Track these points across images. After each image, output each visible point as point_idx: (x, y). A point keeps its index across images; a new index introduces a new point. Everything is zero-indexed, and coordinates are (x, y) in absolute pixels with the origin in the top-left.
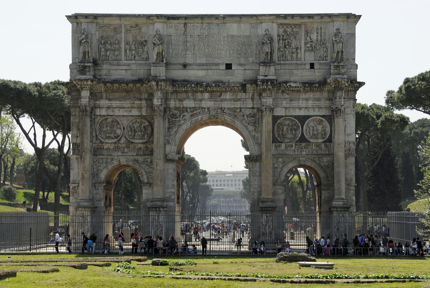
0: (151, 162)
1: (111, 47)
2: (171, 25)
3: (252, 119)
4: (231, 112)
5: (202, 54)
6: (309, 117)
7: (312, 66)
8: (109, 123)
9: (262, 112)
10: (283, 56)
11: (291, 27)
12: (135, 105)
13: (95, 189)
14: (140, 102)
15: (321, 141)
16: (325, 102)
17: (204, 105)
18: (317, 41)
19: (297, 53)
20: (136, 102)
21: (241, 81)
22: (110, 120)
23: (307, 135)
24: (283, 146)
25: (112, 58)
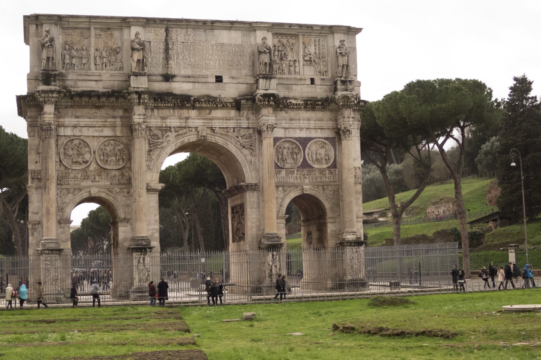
0: (128, 193)
1: (77, 53)
2: (149, 29)
3: (248, 140)
4: (223, 133)
5: (187, 63)
6: (310, 139)
7: (312, 80)
8: (75, 145)
9: (260, 132)
10: (279, 69)
11: (287, 37)
12: (108, 123)
13: (61, 227)
14: (114, 120)
15: (325, 166)
16: (328, 122)
17: (191, 124)
18: (316, 54)
19: (295, 67)
20: (108, 120)
21: (234, 96)
22: (76, 142)
23: (309, 160)
24: (283, 172)
25: (78, 67)
